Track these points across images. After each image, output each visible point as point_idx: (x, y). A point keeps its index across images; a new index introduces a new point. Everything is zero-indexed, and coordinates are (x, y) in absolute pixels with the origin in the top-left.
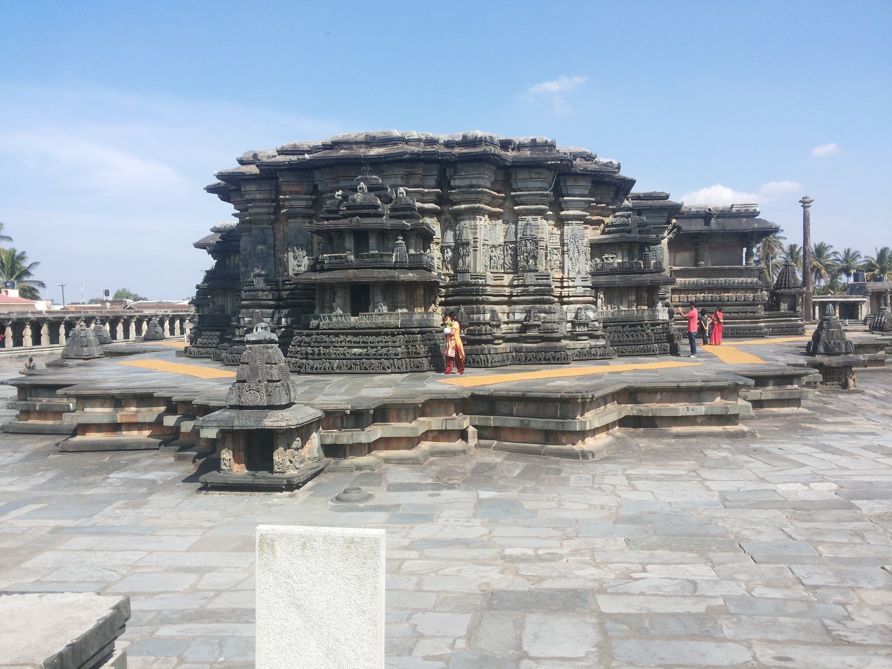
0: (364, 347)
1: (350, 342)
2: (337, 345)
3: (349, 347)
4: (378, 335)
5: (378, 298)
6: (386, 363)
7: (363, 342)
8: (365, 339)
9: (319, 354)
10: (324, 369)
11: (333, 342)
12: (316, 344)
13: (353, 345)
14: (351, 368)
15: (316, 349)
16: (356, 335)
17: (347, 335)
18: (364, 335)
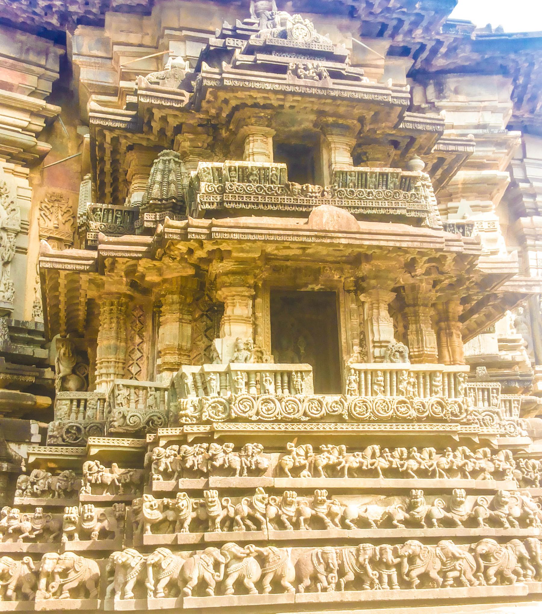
0: (389, 492)
1: (333, 470)
2: (280, 482)
3: (333, 492)
4: (442, 443)
5: (384, 329)
6: (507, 557)
7: (391, 472)
8: (395, 458)
9: (202, 523)
10: (241, 587)
11: (258, 471)
12: (186, 483)
13: (345, 482)
14: (358, 583)
15: (186, 504)
16: (356, 444)
17: (317, 442)
18: (389, 443)
